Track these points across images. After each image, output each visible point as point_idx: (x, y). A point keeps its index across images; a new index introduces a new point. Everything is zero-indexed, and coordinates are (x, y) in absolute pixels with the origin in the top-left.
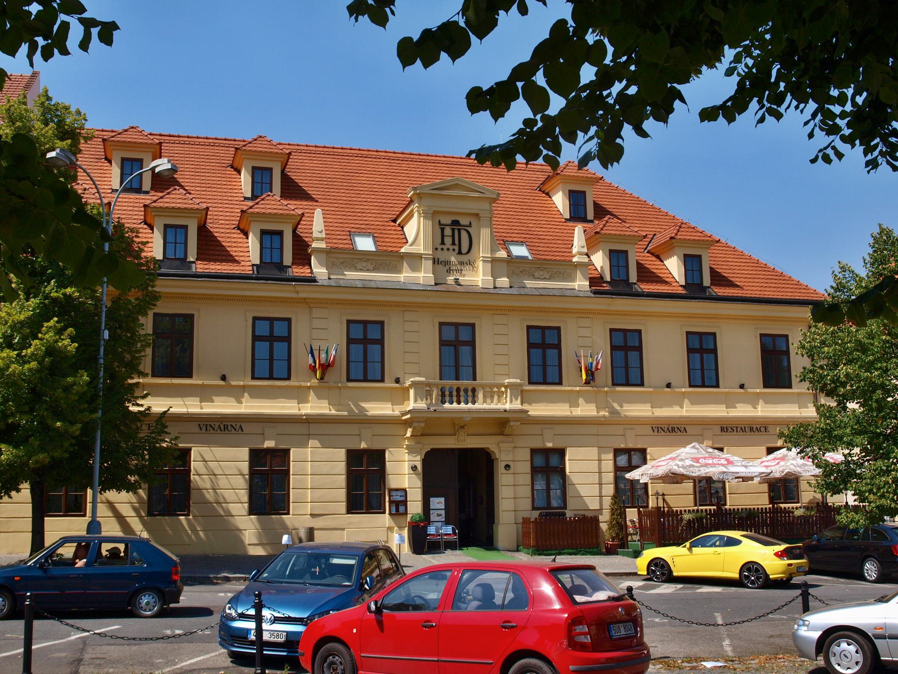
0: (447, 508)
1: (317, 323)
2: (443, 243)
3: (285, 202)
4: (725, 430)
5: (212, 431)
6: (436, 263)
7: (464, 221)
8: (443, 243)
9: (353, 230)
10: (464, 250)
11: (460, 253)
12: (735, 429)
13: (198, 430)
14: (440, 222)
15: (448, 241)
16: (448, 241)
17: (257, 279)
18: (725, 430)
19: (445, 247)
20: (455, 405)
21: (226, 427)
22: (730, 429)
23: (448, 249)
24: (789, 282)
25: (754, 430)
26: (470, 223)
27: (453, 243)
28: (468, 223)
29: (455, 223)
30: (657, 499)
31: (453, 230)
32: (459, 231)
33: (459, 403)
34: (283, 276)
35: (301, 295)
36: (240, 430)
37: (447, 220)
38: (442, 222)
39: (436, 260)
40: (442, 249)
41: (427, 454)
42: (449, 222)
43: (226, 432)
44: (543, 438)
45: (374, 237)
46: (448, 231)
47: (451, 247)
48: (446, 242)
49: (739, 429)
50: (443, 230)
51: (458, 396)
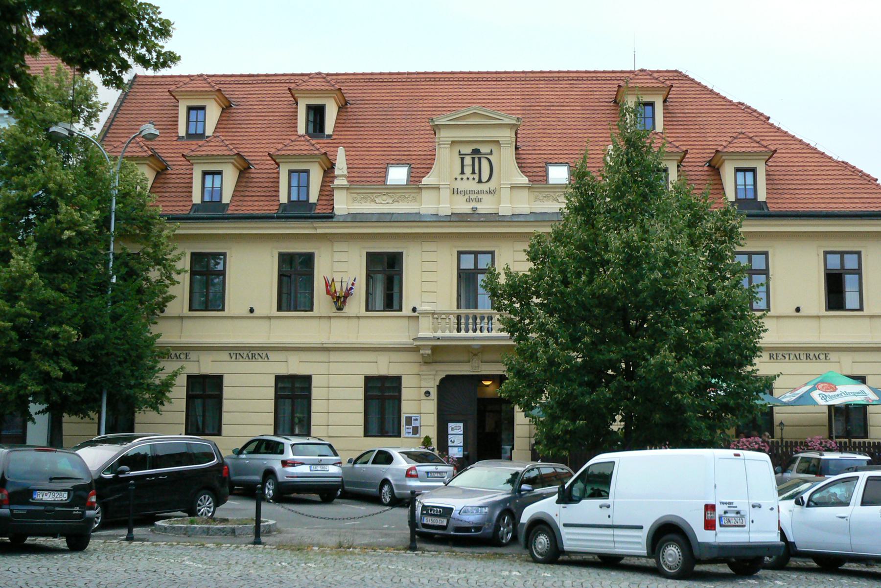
0: (465, 435)
1: (337, 257)
2: (462, 173)
3: (313, 142)
4: (775, 357)
5: (241, 359)
6: (455, 193)
7: (484, 149)
8: (462, 173)
9: (392, 162)
10: (485, 177)
11: (480, 181)
12: (787, 357)
13: (228, 358)
14: (460, 152)
15: (468, 170)
16: (468, 170)
17: (278, 218)
18: (775, 357)
19: (465, 177)
20: (471, 334)
21: (253, 356)
22: (780, 357)
23: (468, 179)
24: (875, 191)
25: (811, 357)
26: (491, 151)
27: (473, 172)
28: (489, 151)
29: (476, 152)
30: (782, 430)
31: (473, 159)
32: (480, 159)
33: (467, 331)
34: (313, 213)
35: (320, 231)
36: (266, 358)
37: (468, 150)
38: (462, 152)
39: (456, 190)
40: (462, 179)
41: (443, 381)
42: (470, 151)
43: (254, 360)
44: (288, 366)
45: (411, 168)
46: (468, 161)
47: (471, 177)
48: (465, 171)
49: (792, 357)
50: (462, 159)
51: (467, 324)
